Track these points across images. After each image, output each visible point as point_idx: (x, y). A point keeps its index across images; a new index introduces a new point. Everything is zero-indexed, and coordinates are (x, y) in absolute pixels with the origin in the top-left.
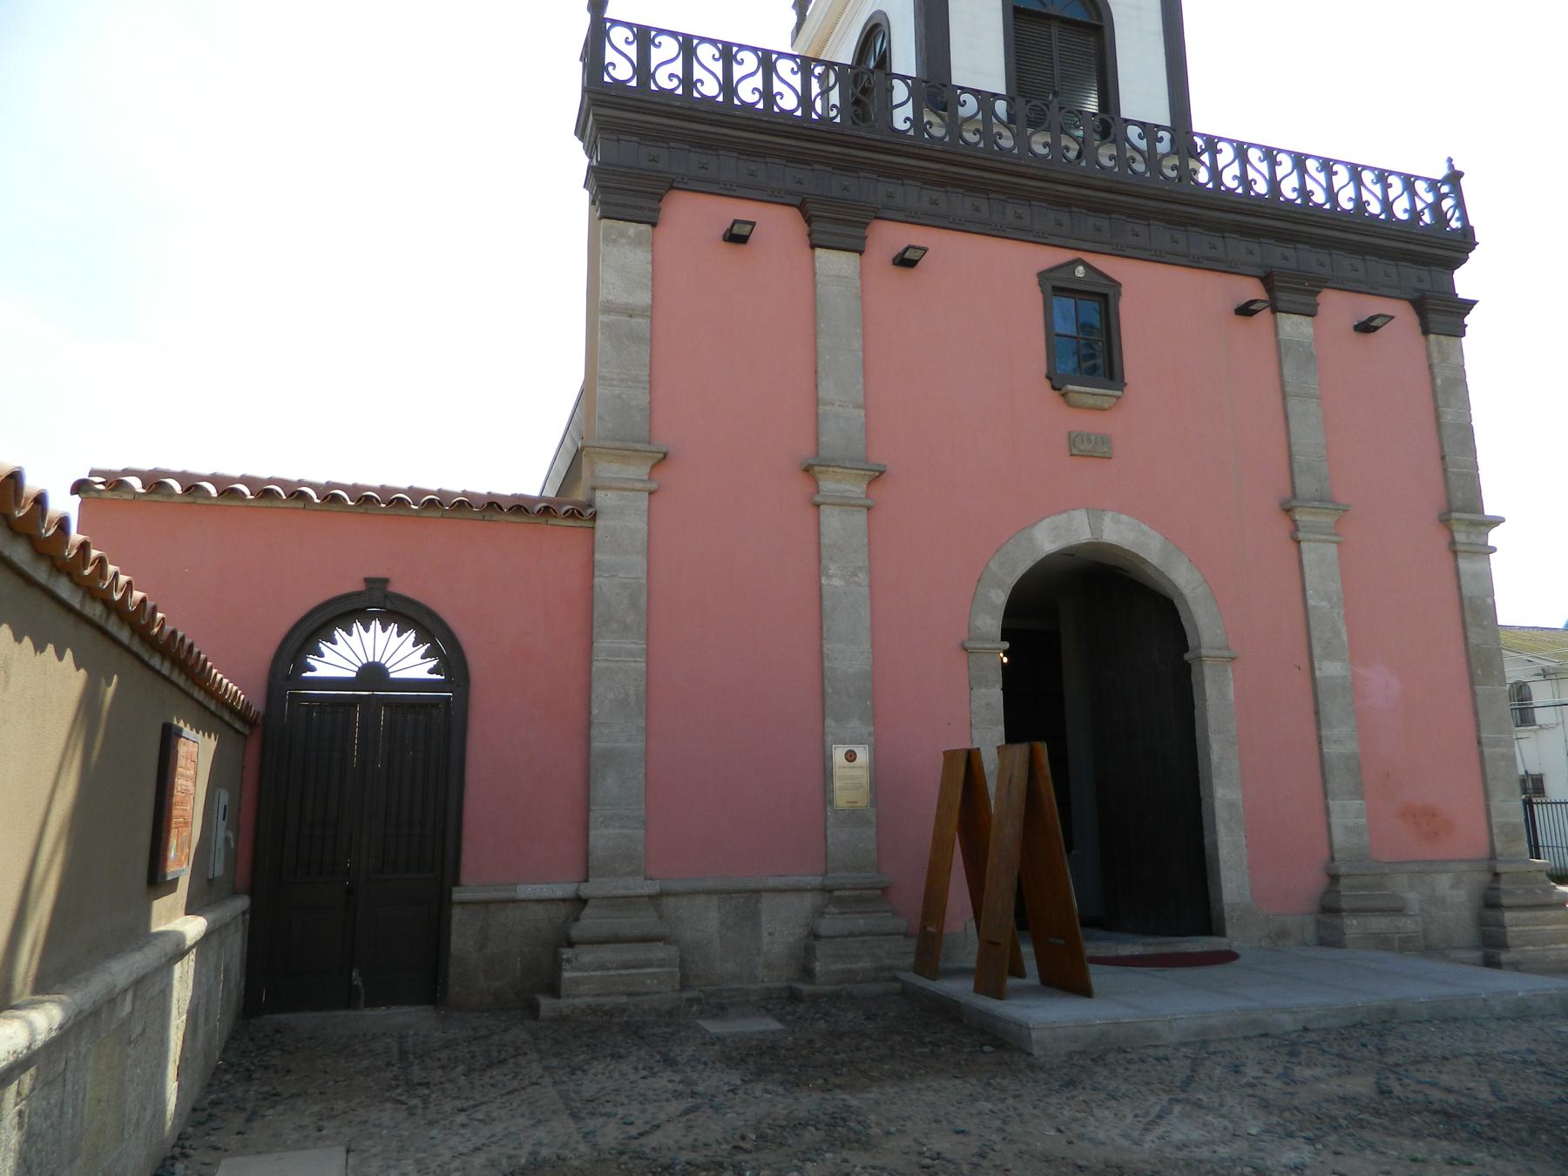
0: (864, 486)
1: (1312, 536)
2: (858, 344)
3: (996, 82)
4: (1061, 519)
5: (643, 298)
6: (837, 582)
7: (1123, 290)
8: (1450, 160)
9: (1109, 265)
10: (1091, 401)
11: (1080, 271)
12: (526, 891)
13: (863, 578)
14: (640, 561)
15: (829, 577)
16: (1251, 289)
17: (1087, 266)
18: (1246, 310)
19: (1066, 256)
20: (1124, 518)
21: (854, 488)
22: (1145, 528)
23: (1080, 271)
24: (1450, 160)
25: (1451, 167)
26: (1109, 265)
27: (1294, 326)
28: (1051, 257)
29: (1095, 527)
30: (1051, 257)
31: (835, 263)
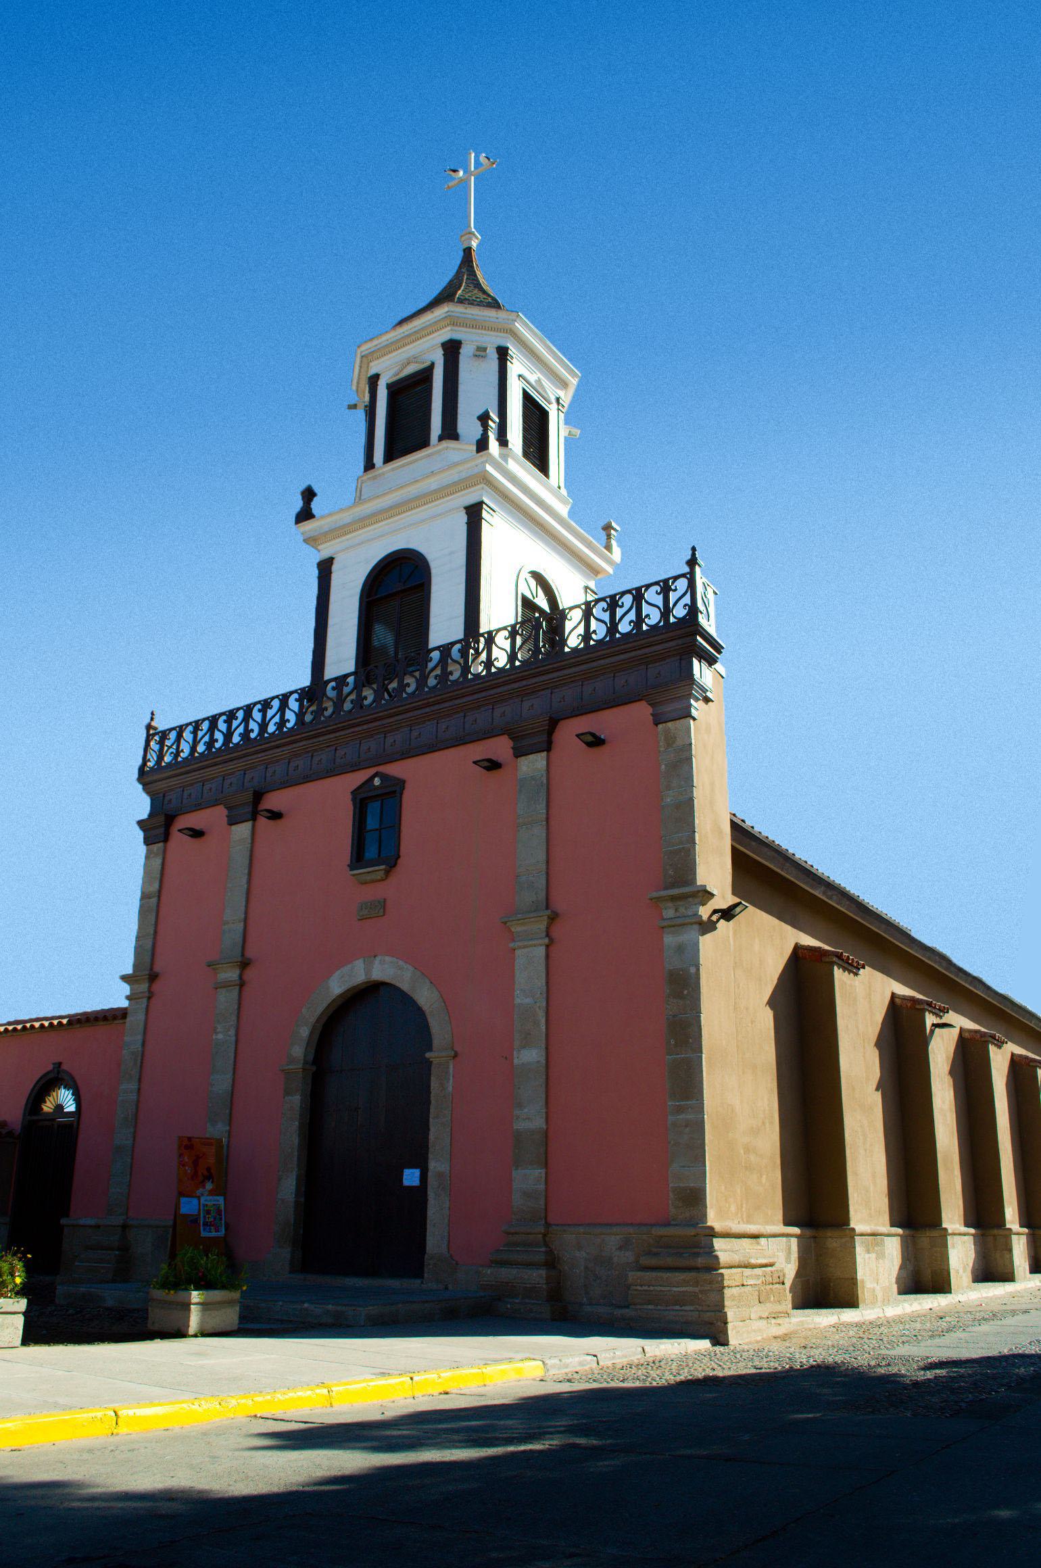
0: (238, 972)
1: (520, 944)
2: (244, 880)
3: (350, 666)
4: (346, 969)
5: (156, 885)
6: (220, 1036)
7: (406, 785)
8: (694, 549)
9: (395, 769)
10: (369, 878)
11: (377, 781)
12: (82, 1222)
13: (232, 1032)
14: (140, 1038)
15: (217, 1033)
16: (500, 747)
17: (384, 777)
18: (492, 765)
19: (372, 771)
20: (387, 958)
21: (232, 974)
22: (401, 963)
23: (377, 781)
24: (694, 549)
25: (694, 554)
26: (395, 769)
27: (534, 764)
28: (359, 778)
29: (368, 971)
30: (359, 778)
31: (243, 830)
